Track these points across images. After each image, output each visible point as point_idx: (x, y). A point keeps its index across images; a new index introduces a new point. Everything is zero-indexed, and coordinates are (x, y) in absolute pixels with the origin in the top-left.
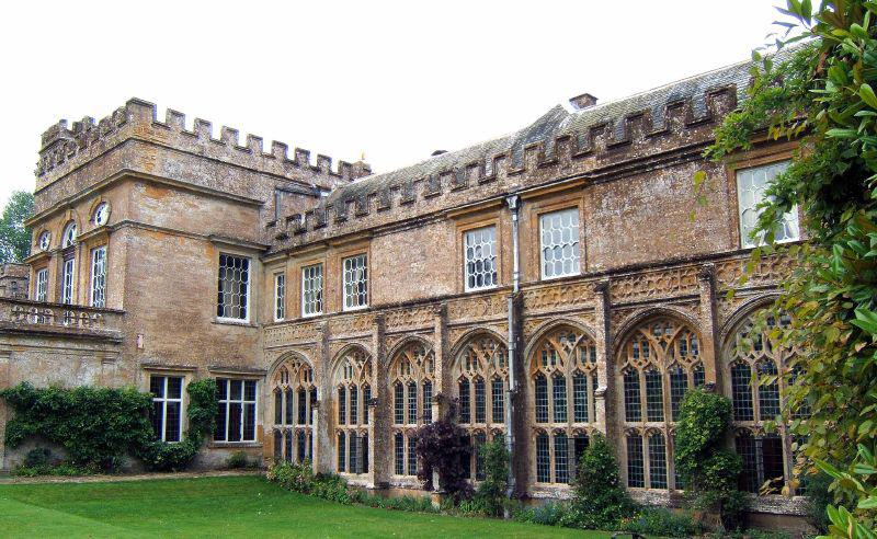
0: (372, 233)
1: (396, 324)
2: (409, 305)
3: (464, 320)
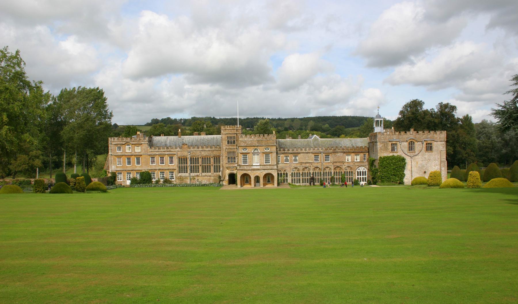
0: (299, 153)
1: (304, 165)
2: (306, 163)
3: (315, 165)
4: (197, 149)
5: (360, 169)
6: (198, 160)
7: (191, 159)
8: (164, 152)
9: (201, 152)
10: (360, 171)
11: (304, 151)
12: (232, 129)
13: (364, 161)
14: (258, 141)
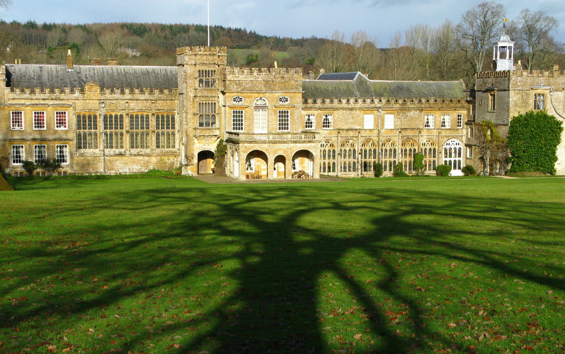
2: (348, 130)
3: (365, 135)
4: (121, 96)
5: (451, 143)
6: (122, 121)
7: (105, 117)
8: (44, 99)
9: (129, 101)
10: (460, 148)
11: (346, 106)
12: (210, 55)
13: (458, 128)
14: (267, 82)
